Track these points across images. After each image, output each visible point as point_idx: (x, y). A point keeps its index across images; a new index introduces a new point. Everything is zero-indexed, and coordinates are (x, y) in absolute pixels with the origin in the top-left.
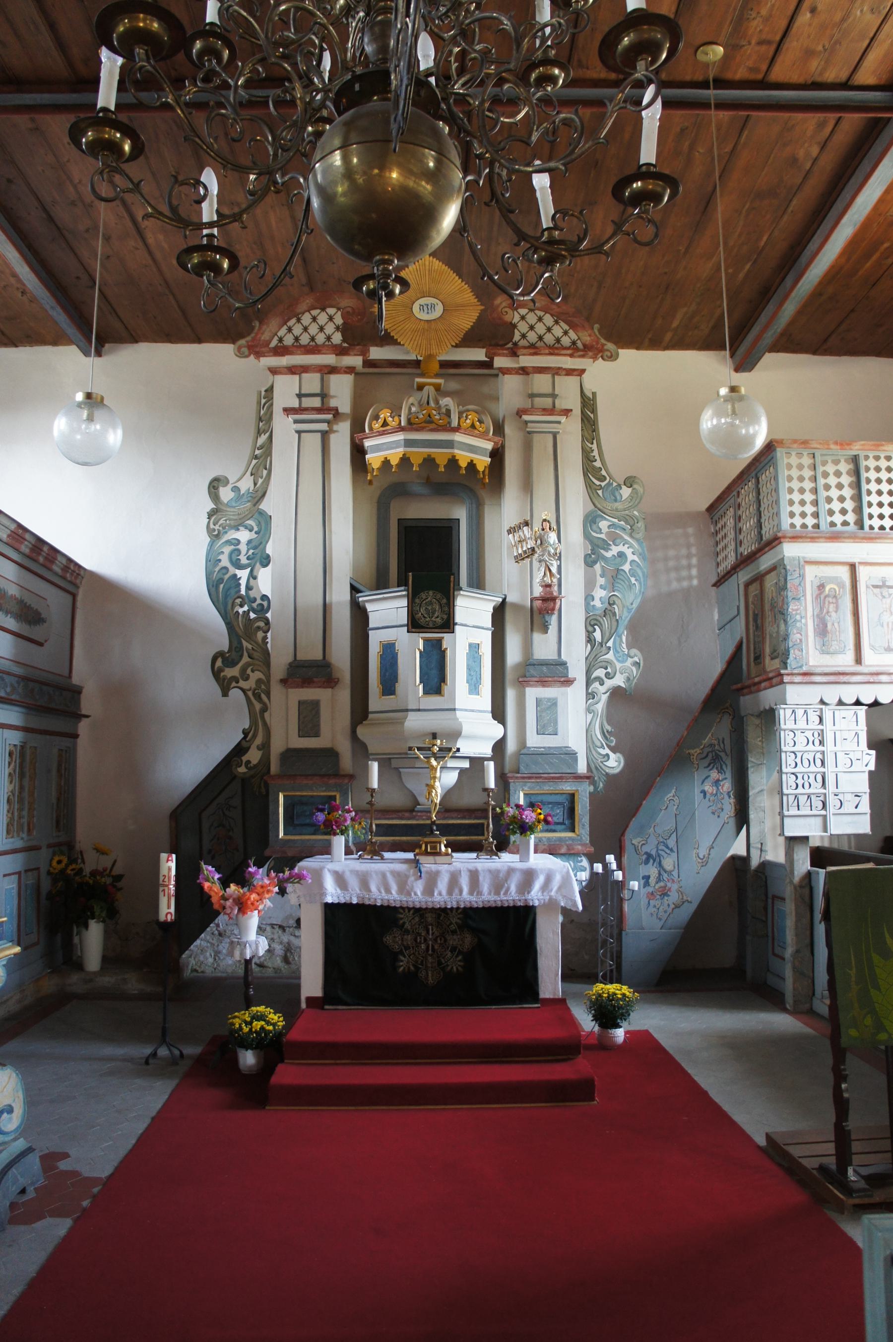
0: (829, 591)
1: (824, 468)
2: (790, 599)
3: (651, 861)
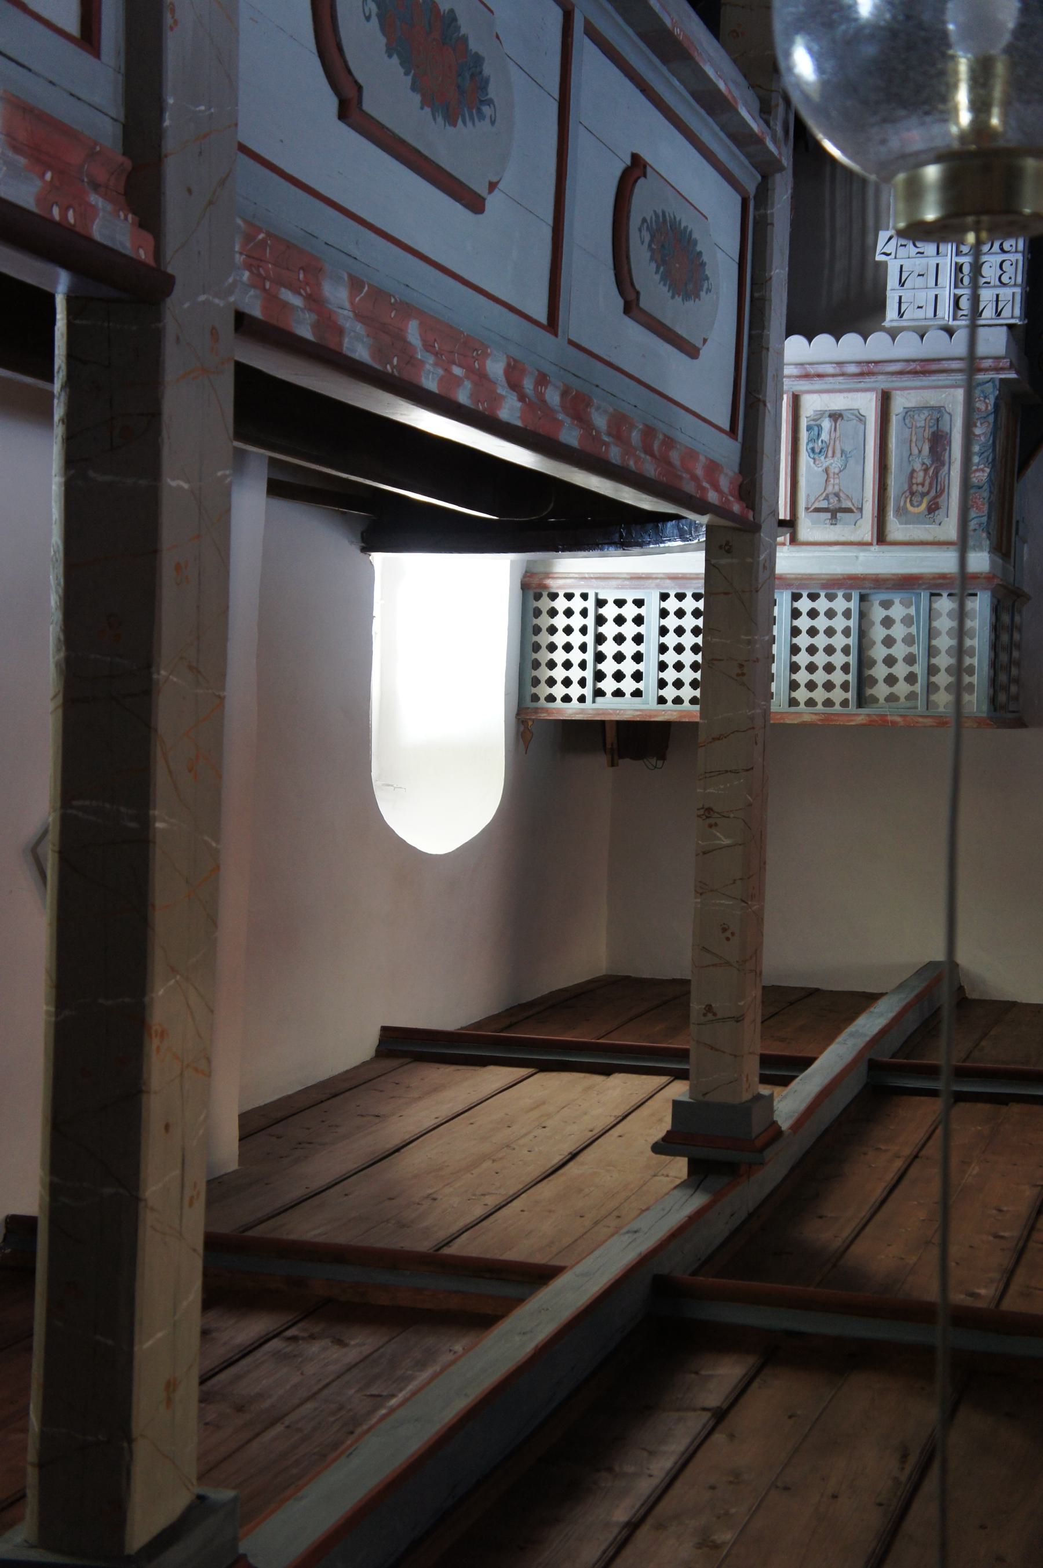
0: (921, 503)
1: (912, 688)
2: (986, 487)
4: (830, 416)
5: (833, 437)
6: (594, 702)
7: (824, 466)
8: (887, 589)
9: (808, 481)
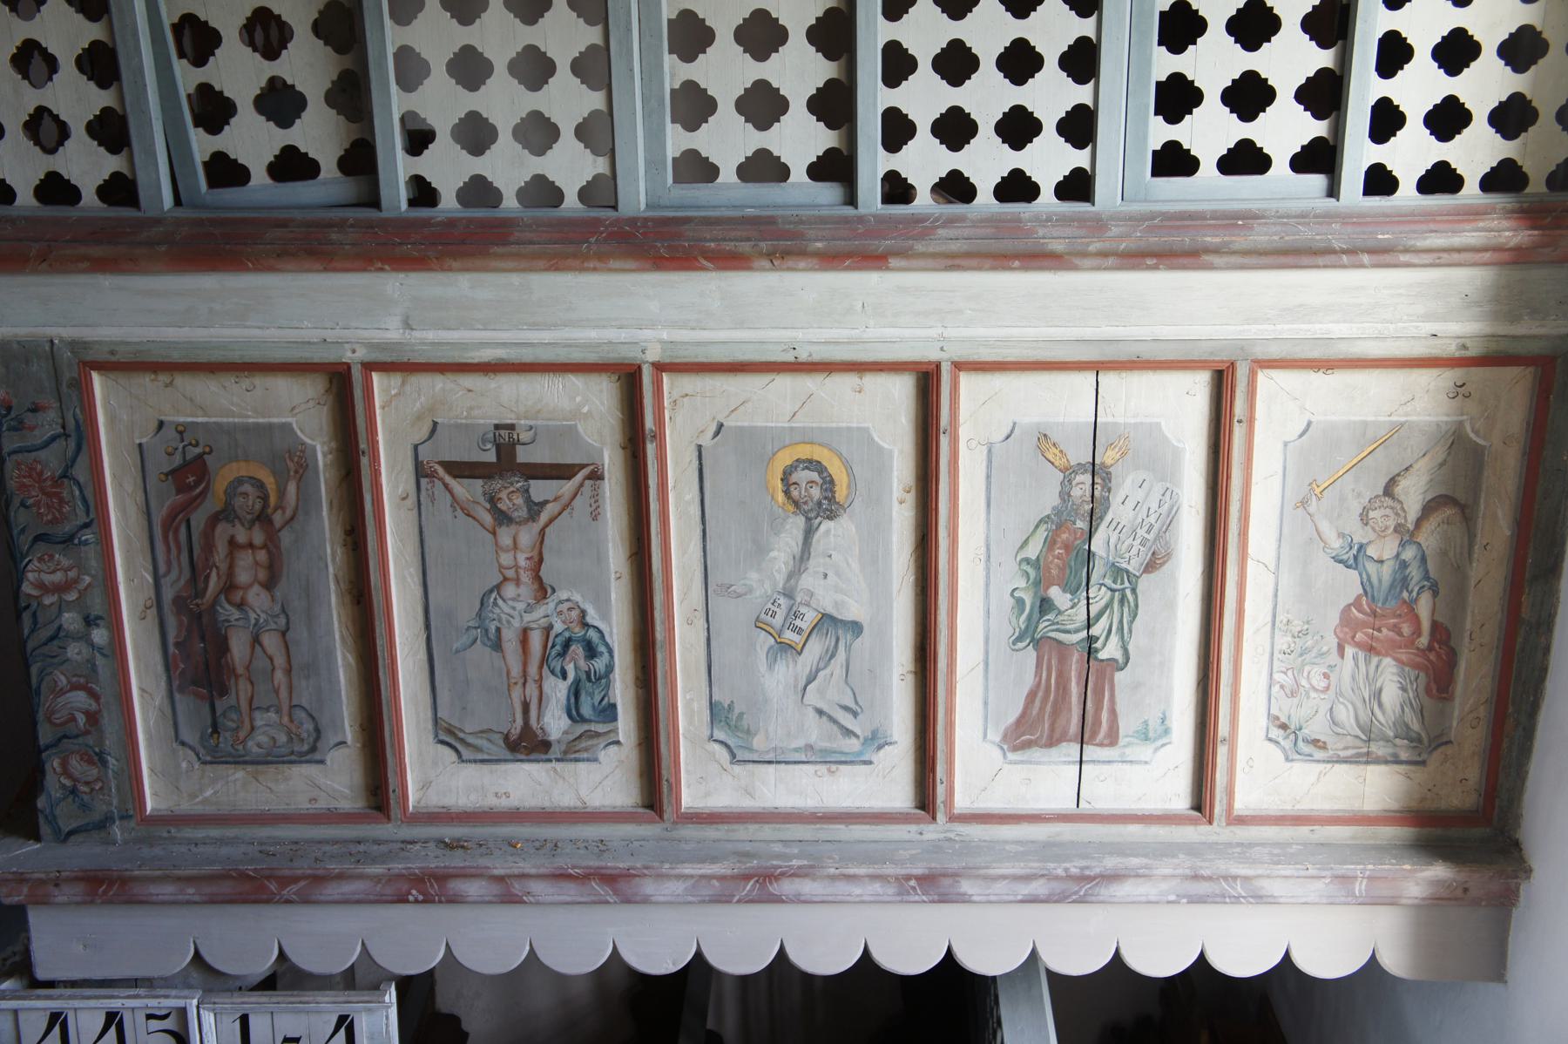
2: (24, 542)
4: (545, 745)
5: (532, 690)
7: (549, 606)
8: (282, 224)
9: (600, 559)
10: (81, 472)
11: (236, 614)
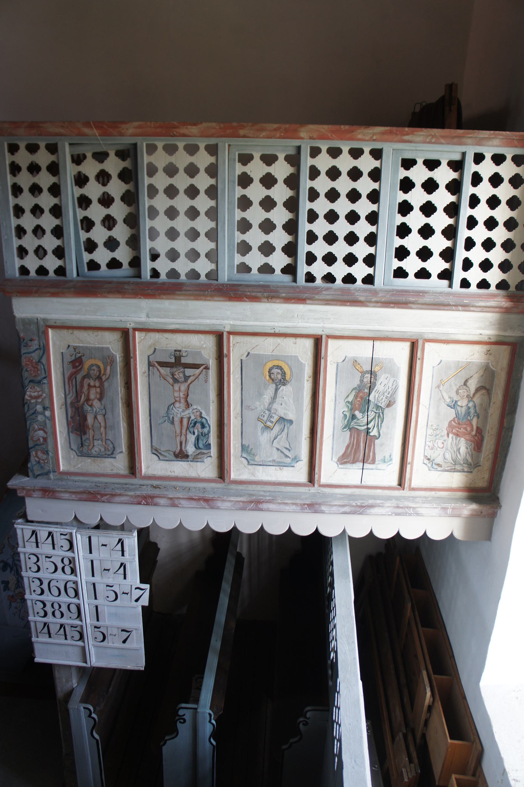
2: (26, 382)
3: (9, 569)
4: (187, 456)
5: (183, 438)
6: (464, 154)
7: (190, 410)
8: (110, 283)
9: (207, 396)
10: (44, 361)
11: (90, 408)
